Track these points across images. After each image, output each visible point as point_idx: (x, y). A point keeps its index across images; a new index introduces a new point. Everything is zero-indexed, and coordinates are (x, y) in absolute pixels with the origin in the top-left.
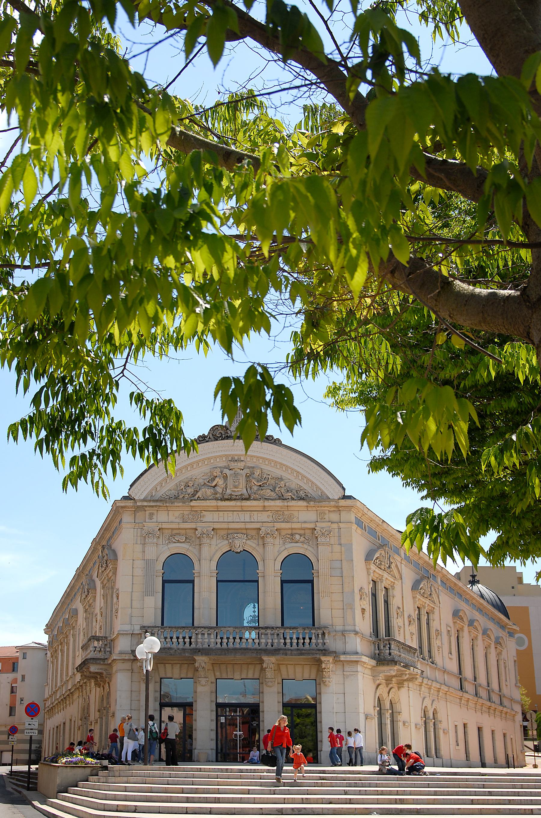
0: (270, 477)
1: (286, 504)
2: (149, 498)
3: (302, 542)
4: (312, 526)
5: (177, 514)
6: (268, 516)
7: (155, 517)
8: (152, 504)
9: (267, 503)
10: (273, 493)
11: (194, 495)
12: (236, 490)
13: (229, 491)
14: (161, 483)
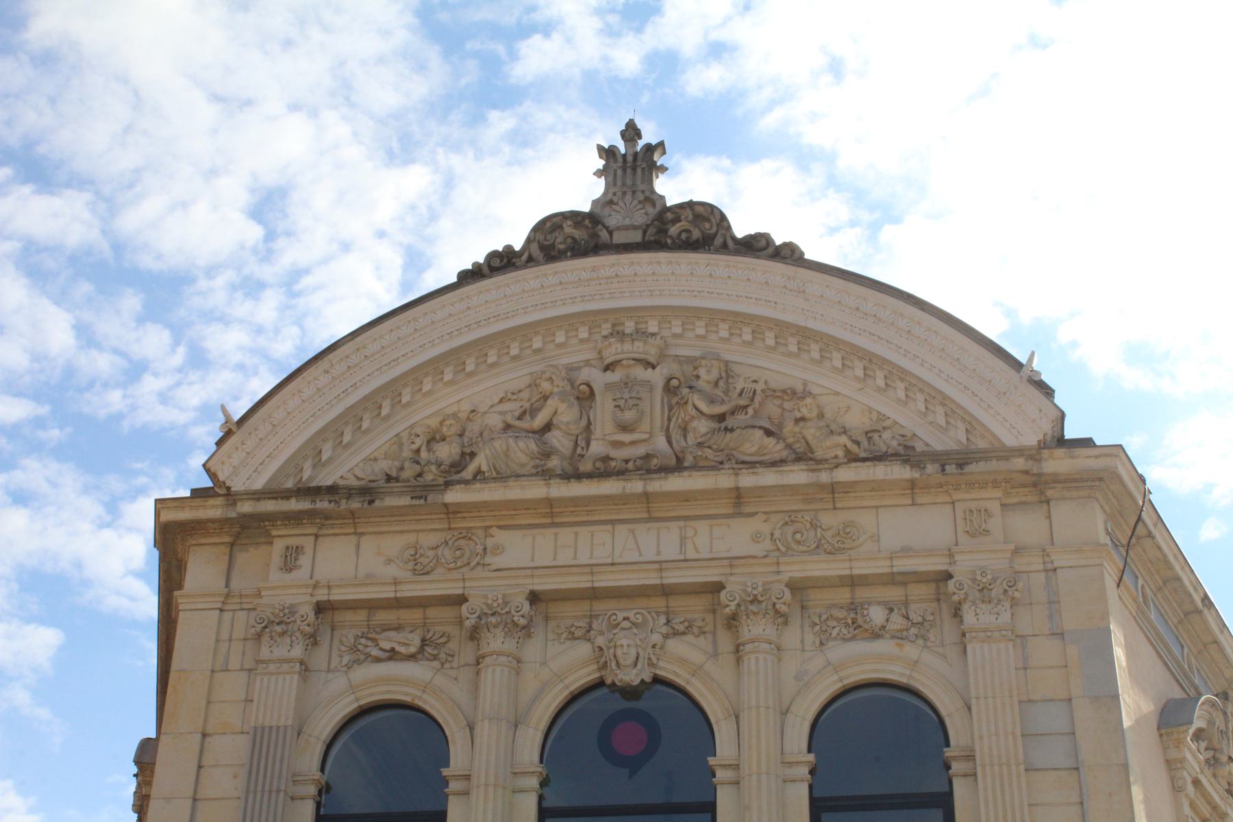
0: (759, 387)
1: (824, 477)
2: (290, 484)
5: (394, 544)
6: (756, 538)
7: (305, 561)
8: (294, 505)
9: (747, 480)
10: (770, 441)
11: (458, 466)
12: (626, 438)
13: (597, 448)
14: (333, 431)
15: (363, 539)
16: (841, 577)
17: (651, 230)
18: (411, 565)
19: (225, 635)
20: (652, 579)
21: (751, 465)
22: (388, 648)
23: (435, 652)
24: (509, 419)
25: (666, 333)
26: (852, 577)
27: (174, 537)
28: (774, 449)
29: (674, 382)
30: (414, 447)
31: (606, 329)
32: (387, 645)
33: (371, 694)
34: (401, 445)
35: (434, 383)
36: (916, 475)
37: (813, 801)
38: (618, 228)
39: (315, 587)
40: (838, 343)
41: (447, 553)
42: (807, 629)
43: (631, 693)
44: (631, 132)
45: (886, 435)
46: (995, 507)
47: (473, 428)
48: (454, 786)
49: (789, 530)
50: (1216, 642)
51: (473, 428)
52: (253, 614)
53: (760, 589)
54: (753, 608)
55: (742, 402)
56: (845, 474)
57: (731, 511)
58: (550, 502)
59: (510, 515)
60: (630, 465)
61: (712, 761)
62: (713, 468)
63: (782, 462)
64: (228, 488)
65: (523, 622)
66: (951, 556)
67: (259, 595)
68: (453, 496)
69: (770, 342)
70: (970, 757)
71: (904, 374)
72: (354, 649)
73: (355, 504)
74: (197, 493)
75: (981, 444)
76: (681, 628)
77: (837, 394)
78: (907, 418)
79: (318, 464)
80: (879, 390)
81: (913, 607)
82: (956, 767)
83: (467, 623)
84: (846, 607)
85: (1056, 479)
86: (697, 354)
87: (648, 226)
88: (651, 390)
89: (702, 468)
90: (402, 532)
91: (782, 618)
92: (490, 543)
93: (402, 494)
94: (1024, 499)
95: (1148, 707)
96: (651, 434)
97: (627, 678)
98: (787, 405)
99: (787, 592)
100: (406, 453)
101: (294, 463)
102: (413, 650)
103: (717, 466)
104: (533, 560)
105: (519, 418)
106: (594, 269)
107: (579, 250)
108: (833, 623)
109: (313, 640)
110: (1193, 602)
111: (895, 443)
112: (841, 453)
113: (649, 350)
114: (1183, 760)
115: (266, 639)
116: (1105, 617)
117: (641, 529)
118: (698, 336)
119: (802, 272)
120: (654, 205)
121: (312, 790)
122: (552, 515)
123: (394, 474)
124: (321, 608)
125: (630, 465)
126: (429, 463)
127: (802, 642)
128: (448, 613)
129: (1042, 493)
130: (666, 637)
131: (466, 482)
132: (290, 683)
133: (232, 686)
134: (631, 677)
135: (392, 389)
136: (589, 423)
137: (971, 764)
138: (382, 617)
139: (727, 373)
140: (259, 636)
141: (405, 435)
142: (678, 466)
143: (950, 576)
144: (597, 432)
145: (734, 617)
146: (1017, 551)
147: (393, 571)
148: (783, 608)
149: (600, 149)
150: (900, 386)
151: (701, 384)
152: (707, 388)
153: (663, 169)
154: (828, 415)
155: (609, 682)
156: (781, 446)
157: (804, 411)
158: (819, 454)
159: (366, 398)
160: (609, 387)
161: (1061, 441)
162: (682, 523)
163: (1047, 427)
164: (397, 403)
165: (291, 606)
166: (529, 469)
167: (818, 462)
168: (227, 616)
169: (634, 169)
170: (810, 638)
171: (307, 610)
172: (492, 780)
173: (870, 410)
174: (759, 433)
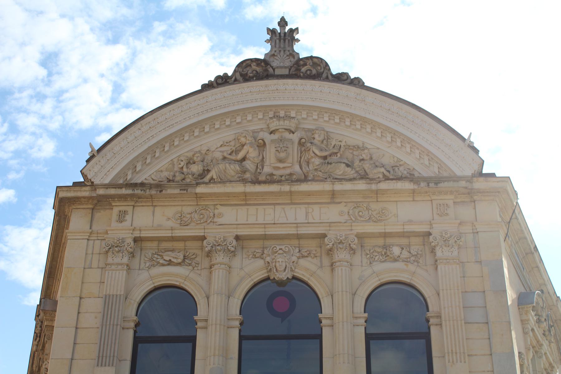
0: (343, 144)
1: (374, 187)
2: (121, 182)
3: (406, 261)
4: (424, 228)
5: (170, 211)
6: (341, 213)
7: (128, 217)
8: (124, 191)
9: (338, 187)
10: (349, 169)
11: (202, 175)
12: (281, 165)
13: (267, 169)
14: (142, 157)
15: (156, 208)
16: (380, 233)
17: (293, 69)
18: (179, 221)
19: (90, 251)
20: (292, 231)
21: (340, 180)
22: (168, 260)
23: (190, 262)
24: (225, 154)
25: (299, 117)
26: (385, 233)
27: (64, 205)
28: (350, 172)
29: (303, 140)
30: (180, 166)
31: (271, 114)
32: (167, 258)
33: (160, 281)
34: (174, 165)
35: (190, 136)
36: (416, 187)
37: (366, 335)
38: (277, 67)
39: (134, 230)
40: (379, 125)
41: (196, 216)
42: (364, 256)
43: (281, 283)
44: (283, 22)
45: (401, 168)
46: (451, 203)
47: (208, 158)
48: (199, 324)
49: (357, 211)
50: (537, 267)
51: (208, 158)
52: (103, 242)
53: (344, 237)
54: (341, 246)
55: (335, 151)
56: (384, 186)
57: (329, 201)
58: (245, 194)
59: (227, 199)
60: (283, 178)
61: (320, 316)
62: (321, 181)
63: (354, 179)
64: (92, 183)
65: (233, 249)
66: (431, 225)
67: (107, 233)
68: (200, 190)
69: (348, 123)
70: (439, 317)
71: (410, 140)
72: (151, 260)
73: (153, 192)
74: (76, 184)
75: (445, 174)
76: (306, 254)
77: (378, 148)
78: (411, 161)
79: (135, 171)
80: (398, 147)
81: (412, 247)
82: (432, 321)
83: (207, 249)
84: (382, 246)
85: (480, 192)
86: (313, 127)
87: (291, 67)
88: (293, 143)
89: (317, 181)
90: (174, 206)
91: (353, 251)
92: (216, 212)
93: (176, 188)
94: (463, 200)
95: (514, 296)
96: (293, 164)
97: (281, 277)
98: (355, 153)
99: (356, 238)
100: (176, 169)
101: (123, 172)
102: (180, 261)
103: (324, 180)
104: (247, 220)
105: (230, 154)
106: (266, 86)
107: (259, 77)
108: (375, 254)
109: (132, 255)
110: (530, 249)
111: (405, 172)
112: (381, 176)
113: (291, 125)
114: (528, 320)
115: (110, 254)
116: (500, 255)
117: (287, 208)
118: (314, 119)
119: (364, 91)
120: (294, 57)
121: (132, 325)
122: (246, 200)
123: (171, 178)
124: (136, 240)
125: (283, 178)
126: (188, 174)
127: (362, 262)
128: (198, 244)
129: (472, 197)
130: (299, 258)
131: (206, 183)
132: (122, 275)
133: (94, 275)
134: (283, 276)
135: (170, 138)
136: (263, 158)
137: (439, 320)
138: (165, 245)
139: (328, 138)
140: (107, 252)
141: (175, 160)
142: (305, 179)
143: (430, 234)
144: (267, 163)
145: (331, 250)
146: (460, 224)
147: (170, 224)
148: (354, 247)
149: (268, 29)
150: (408, 146)
151: (315, 141)
152: (319, 143)
153: (298, 40)
154: (374, 157)
155: (272, 278)
156: (353, 172)
157: (364, 156)
158: (371, 176)
159: (158, 142)
160: (272, 141)
161: (481, 174)
162: (307, 206)
163: (476, 167)
164: (172, 145)
165: (123, 238)
166: (236, 178)
167: (372, 179)
168: (91, 242)
169: (285, 40)
170: (365, 260)
171: (130, 241)
172: (218, 322)
173: (394, 157)
174: (343, 165)
